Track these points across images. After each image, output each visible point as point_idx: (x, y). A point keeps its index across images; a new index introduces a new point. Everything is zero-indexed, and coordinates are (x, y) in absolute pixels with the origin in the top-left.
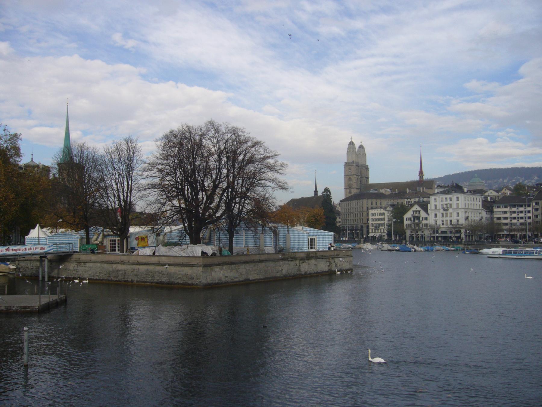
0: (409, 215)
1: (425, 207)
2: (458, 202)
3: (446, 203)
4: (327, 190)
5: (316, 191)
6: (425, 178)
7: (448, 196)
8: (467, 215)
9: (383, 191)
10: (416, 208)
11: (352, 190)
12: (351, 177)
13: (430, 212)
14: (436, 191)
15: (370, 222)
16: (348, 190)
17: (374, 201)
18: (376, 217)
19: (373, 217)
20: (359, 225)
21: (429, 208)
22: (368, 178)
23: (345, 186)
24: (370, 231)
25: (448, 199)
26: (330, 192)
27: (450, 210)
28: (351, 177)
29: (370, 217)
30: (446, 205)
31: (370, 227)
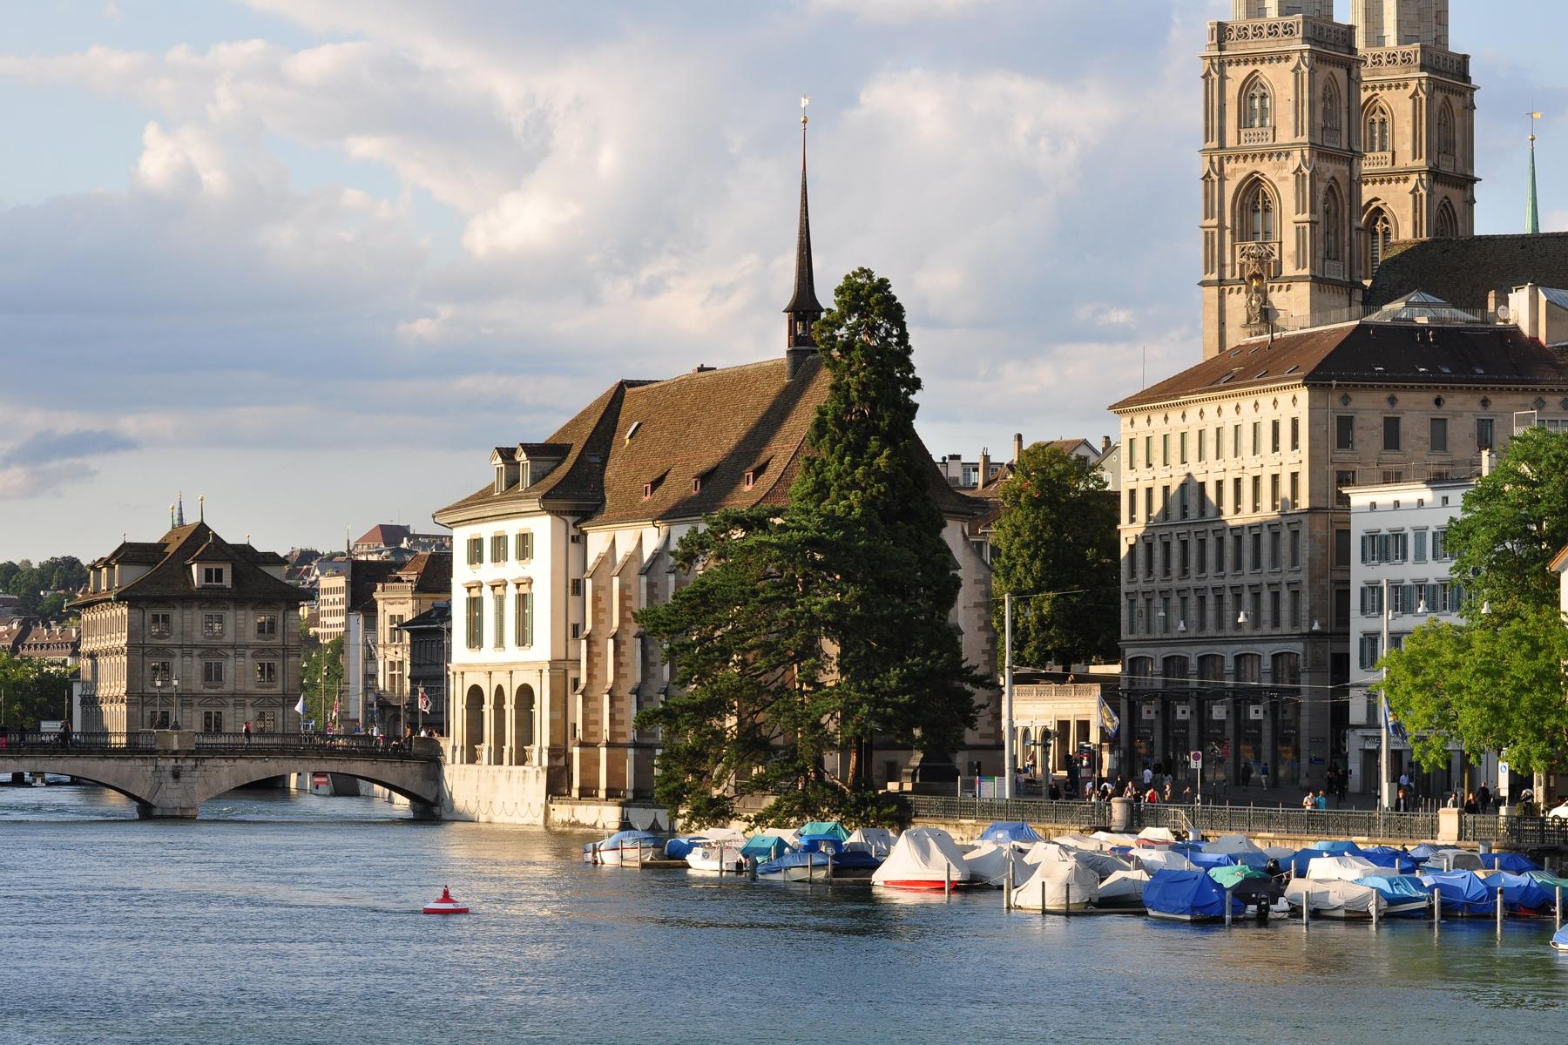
4: (872, 299)
5: (803, 307)
9: (1520, 309)
11: (1277, 298)
12: (1266, 168)
15: (1359, 625)
16: (1238, 303)
17: (1415, 409)
18: (1408, 572)
19: (1385, 573)
20: (1266, 651)
22: (1467, 182)
23: (1214, 258)
24: (1357, 714)
26: (895, 313)
28: (1266, 168)
29: (1360, 573)
31: (1356, 674)
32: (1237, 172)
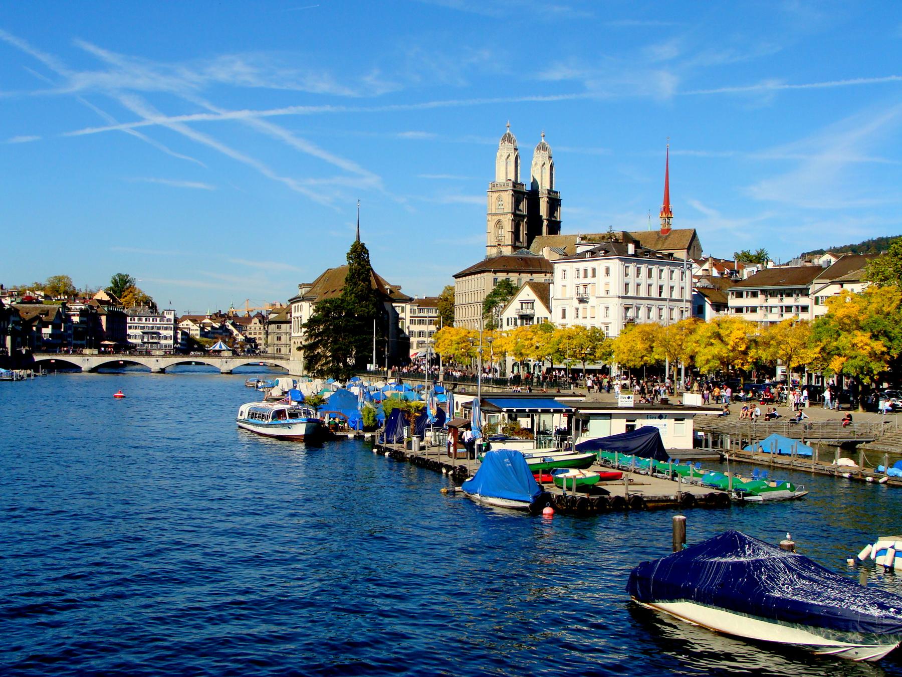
0: (512, 310)
1: (543, 292)
2: (607, 279)
3: (585, 281)
6: (676, 224)
7: (589, 265)
8: (631, 314)
10: (527, 293)
12: (501, 218)
13: (553, 303)
14: (580, 250)
21: (551, 296)
25: (590, 273)
26: (367, 252)
27: (592, 301)
30: (585, 286)
32: (496, 218)
